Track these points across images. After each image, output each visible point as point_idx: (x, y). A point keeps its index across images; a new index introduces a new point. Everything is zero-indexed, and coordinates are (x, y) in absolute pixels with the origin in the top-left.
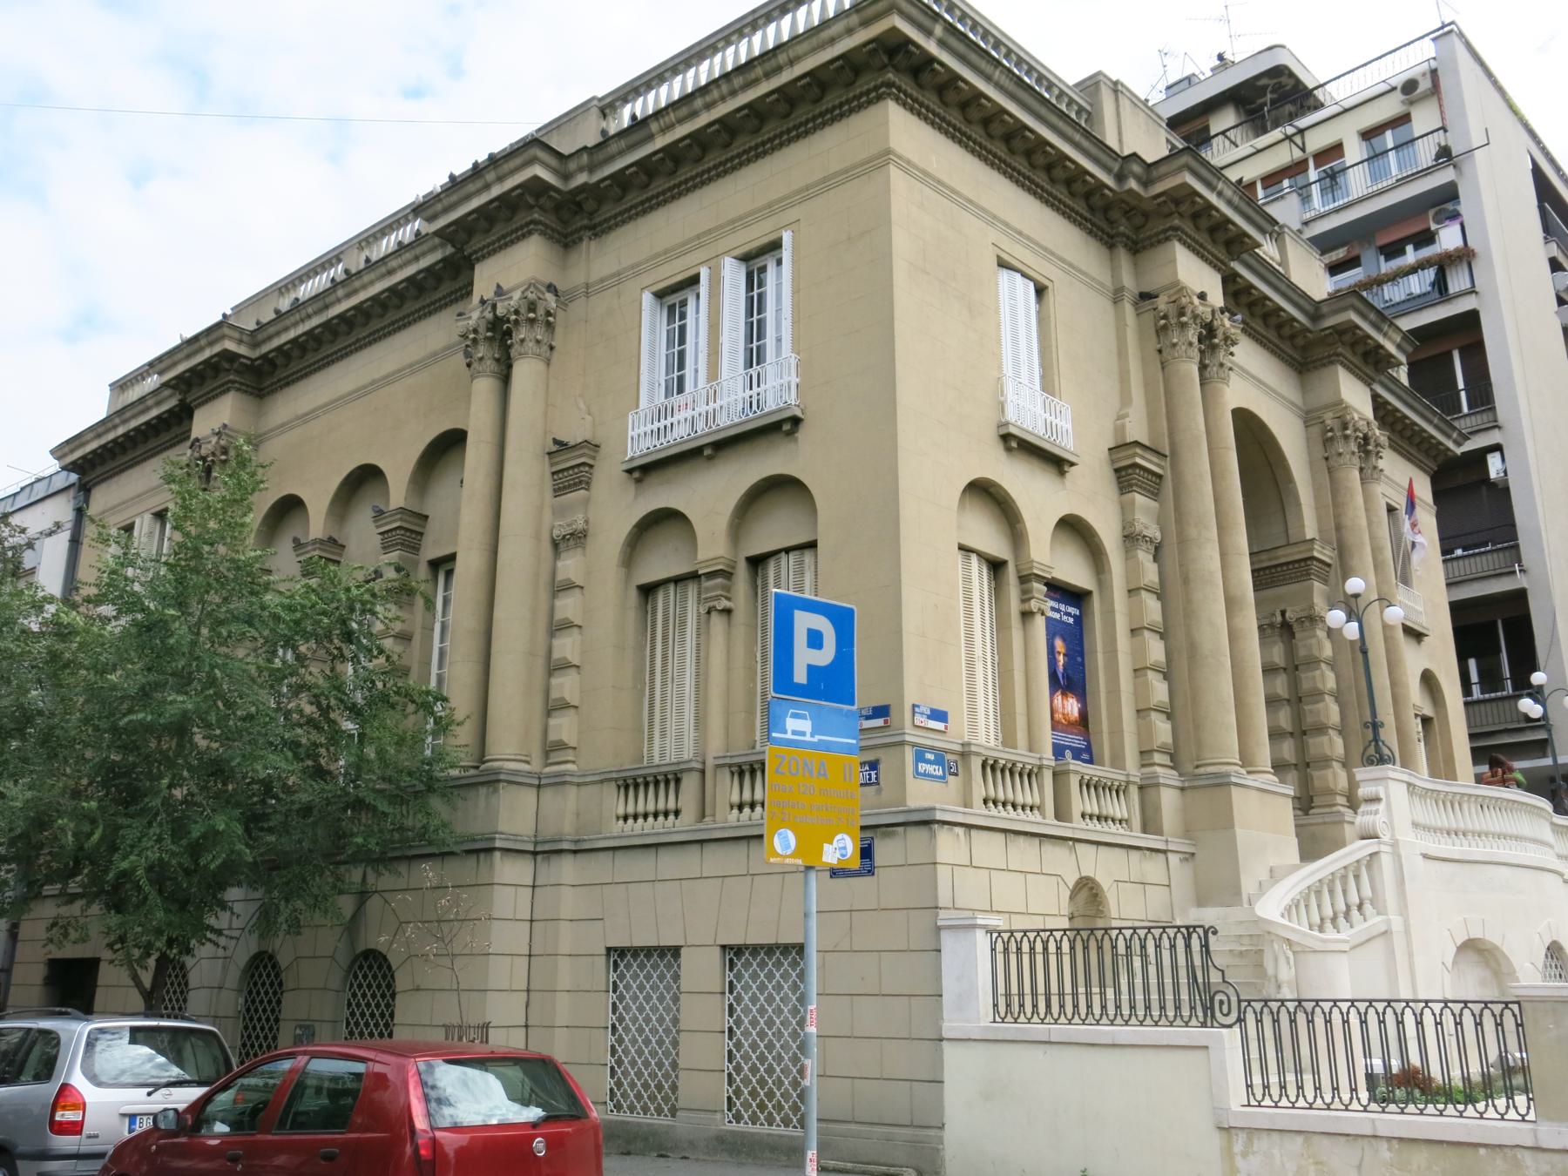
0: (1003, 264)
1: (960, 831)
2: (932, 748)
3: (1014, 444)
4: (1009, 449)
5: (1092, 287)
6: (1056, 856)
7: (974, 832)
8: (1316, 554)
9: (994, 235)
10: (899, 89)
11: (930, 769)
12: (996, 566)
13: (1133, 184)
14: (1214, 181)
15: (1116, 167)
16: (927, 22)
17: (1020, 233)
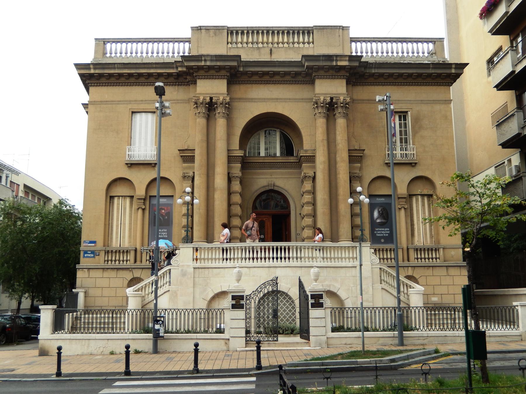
0: (133, 112)
1: (86, 270)
2: (89, 251)
3: (129, 165)
4: (129, 167)
5: (178, 103)
6: (121, 273)
7: (91, 270)
8: (302, 155)
9: (130, 106)
10: (91, 83)
11: (89, 255)
12: (132, 197)
13: (180, 69)
14: (200, 59)
15: (175, 66)
16: (87, 67)
17: (142, 101)
